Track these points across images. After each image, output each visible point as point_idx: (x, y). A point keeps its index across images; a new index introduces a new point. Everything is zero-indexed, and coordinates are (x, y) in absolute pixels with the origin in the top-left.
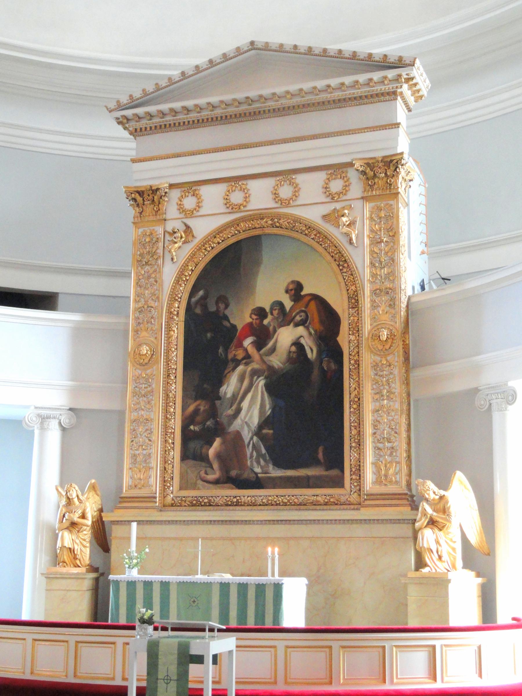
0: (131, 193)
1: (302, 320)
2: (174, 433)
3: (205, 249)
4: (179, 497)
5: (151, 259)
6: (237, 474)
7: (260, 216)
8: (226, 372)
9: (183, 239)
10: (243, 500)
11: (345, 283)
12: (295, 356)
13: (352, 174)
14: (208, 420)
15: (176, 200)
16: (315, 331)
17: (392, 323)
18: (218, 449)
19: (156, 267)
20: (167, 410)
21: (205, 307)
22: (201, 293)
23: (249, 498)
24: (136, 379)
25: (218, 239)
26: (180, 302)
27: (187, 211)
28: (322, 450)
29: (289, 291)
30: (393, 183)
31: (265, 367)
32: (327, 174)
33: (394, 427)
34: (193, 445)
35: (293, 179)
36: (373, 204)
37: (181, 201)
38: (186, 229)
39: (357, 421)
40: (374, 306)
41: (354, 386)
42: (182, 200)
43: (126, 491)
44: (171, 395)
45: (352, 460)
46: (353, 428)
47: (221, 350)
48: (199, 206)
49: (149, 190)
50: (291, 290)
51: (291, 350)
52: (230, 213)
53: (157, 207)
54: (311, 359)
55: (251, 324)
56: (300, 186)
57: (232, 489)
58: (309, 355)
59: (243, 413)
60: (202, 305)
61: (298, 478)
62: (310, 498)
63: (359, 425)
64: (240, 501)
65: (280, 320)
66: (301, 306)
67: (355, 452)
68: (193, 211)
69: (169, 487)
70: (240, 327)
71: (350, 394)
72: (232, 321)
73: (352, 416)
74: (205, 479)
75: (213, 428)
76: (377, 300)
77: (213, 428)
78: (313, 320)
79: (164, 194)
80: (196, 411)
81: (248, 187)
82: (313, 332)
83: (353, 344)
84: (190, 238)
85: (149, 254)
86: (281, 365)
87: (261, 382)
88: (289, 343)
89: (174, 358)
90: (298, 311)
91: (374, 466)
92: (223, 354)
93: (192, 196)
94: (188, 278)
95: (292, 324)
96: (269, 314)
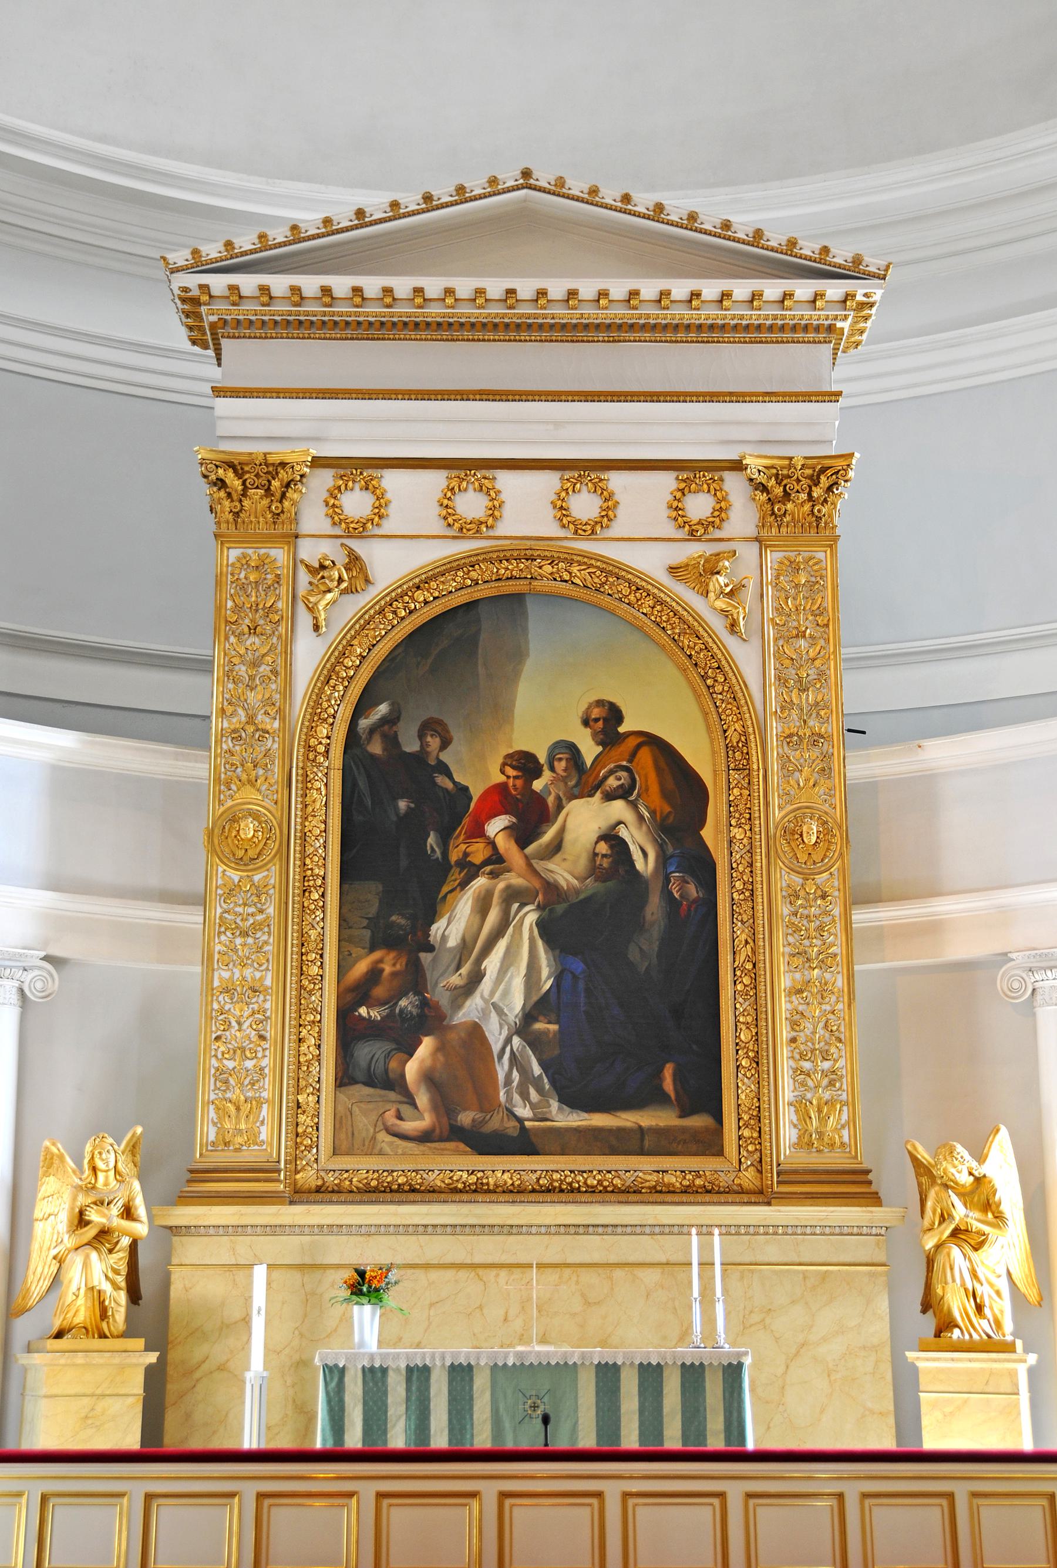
0: (217, 467)
1: (623, 784)
2: (320, 1021)
3: (395, 613)
4: (334, 1171)
5: (262, 622)
6: (473, 1120)
8: (445, 889)
9: (344, 585)
10: (491, 1181)
11: (719, 715)
12: (606, 863)
13: (734, 484)
14: (403, 994)
15: (325, 495)
16: (653, 813)
17: (826, 807)
18: (428, 1063)
19: (275, 640)
20: (302, 970)
21: (392, 742)
22: (383, 709)
23: (506, 1176)
25: (425, 593)
26: (332, 724)
27: (352, 522)
28: (671, 1071)
29: (592, 723)
30: (824, 515)
31: (537, 884)
32: (677, 478)
33: (834, 1028)
34: (366, 1052)
35: (601, 480)
36: (778, 555)
37: (335, 498)
38: (350, 562)
39: (753, 1012)
40: (788, 768)
41: (743, 937)
42: (339, 495)
43: (201, 1155)
44: (313, 934)
45: (743, 1096)
46: (743, 1027)
47: (432, 840)
48: (380, 512)
49: (261, 465)
50: (596, 720)
51: (597, 851)
52: (454, 538)
53: (279, 505)
54: (645, 874)
55: (501, 789)
56: (616, 498)
57: (465, 1153)
58: (640, 865)
60: (385, 737)
61: (619, 1132)
62: (648, 1177)
64: (485, 1181)
65: (571, 783)
66: (620, 754)
67: (749, 1078)
68: (365, 524)
69: (311, 1147)
70: (476, 792)
71: (734, 953)
73: (741, 1000)
74: (396, 1129)
75: (415, 1013)
76: (794, 755)
77: (415, 1013)
78: (647, 790)
79: (298, 478)
80: (374, 975)
81: (498, 486)
82: (646, 814)
83: (741, 846)
84: (360, 584)
85: (257, 611)
86: (575, 882)
87: (530, 917)
88: (595, 839)
89: (320, 851)
90: (612, 765)
91: (792, 1109)
92: (437, 849)
93: (361, 489)
94: (352, 673)
95: (598, 795)
96: (545, 768)
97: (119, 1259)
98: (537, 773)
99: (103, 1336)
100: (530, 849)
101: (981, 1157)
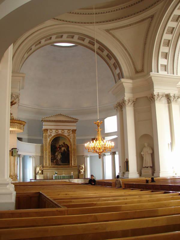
7: (60, 134)
87: (60, 154)
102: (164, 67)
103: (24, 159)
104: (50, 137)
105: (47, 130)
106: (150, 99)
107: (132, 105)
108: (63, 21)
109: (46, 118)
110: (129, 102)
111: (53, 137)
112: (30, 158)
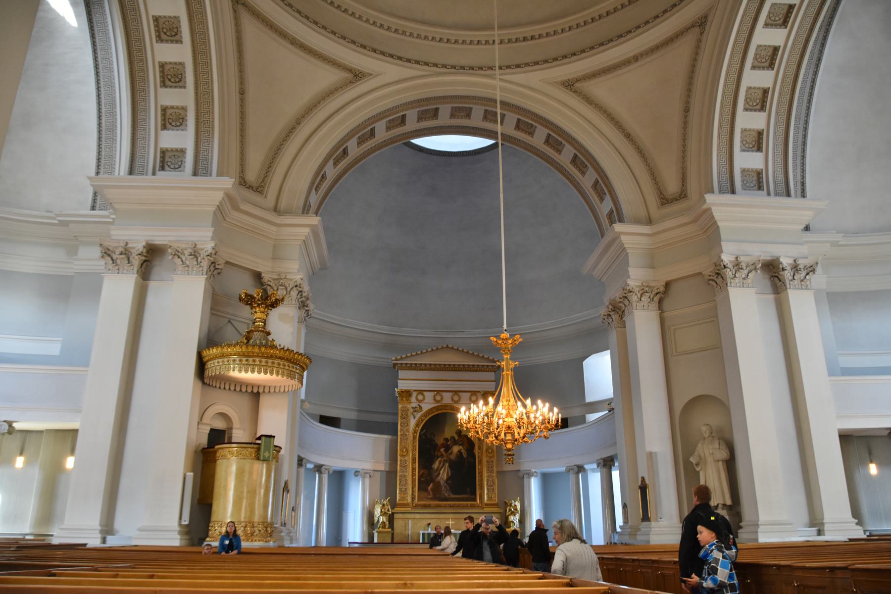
22: (424, 431)
24: (401, 461)
55: (443, 443)
59: (441, 475)
63: (482, 481)
70: (439, 444)
72: (437, 442)
80: (423, 473)
97: (387, 517)
98: (448, 441)
99: (385, 528)
100: (447, 453)
101: (515, 502)
102: (755, 178)
103: (339, 479)
104: (418, 415)
105: (407, 394)
106: (712, 280)
107: (655, 305)
108: (436, 65)
109: (407, 357)
110: (641, 296)
111: (426, 415)
112: (356, 476)
